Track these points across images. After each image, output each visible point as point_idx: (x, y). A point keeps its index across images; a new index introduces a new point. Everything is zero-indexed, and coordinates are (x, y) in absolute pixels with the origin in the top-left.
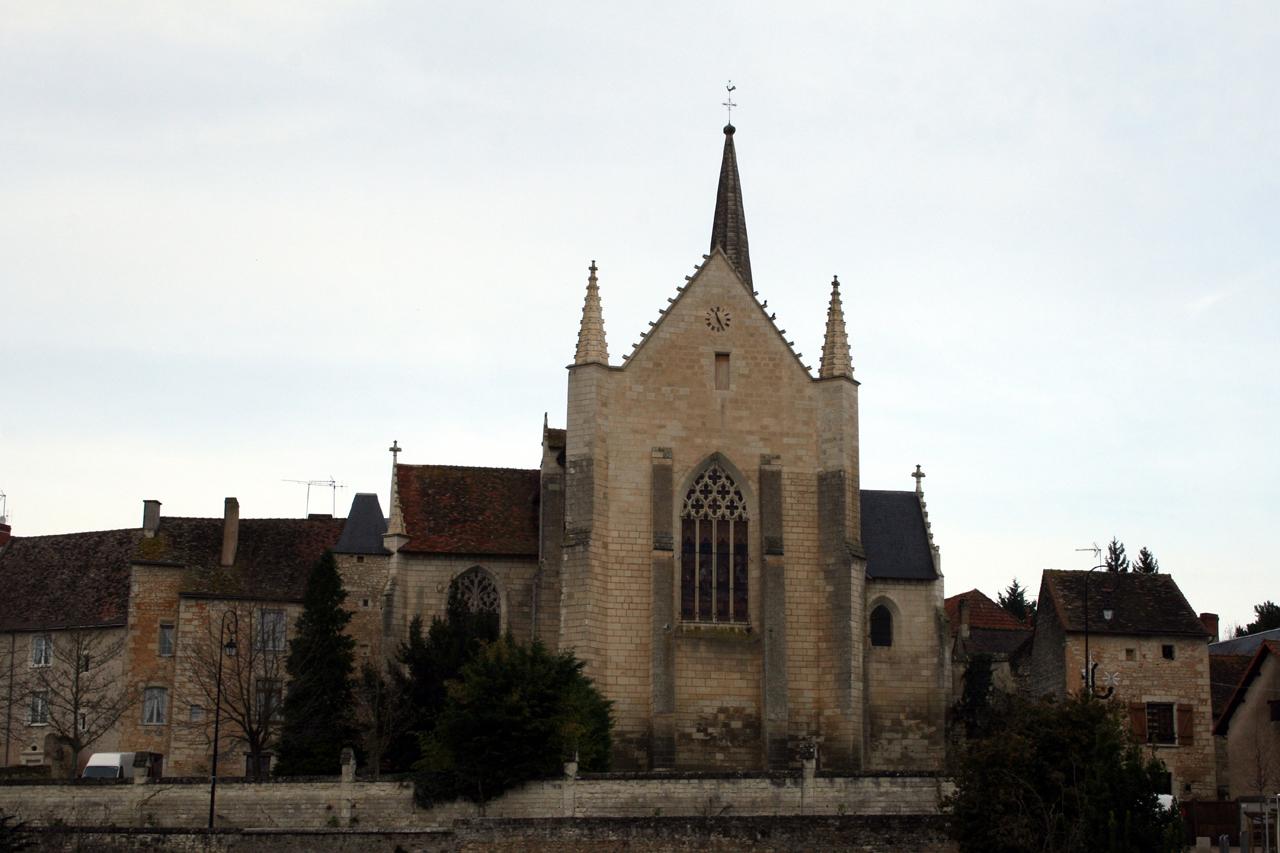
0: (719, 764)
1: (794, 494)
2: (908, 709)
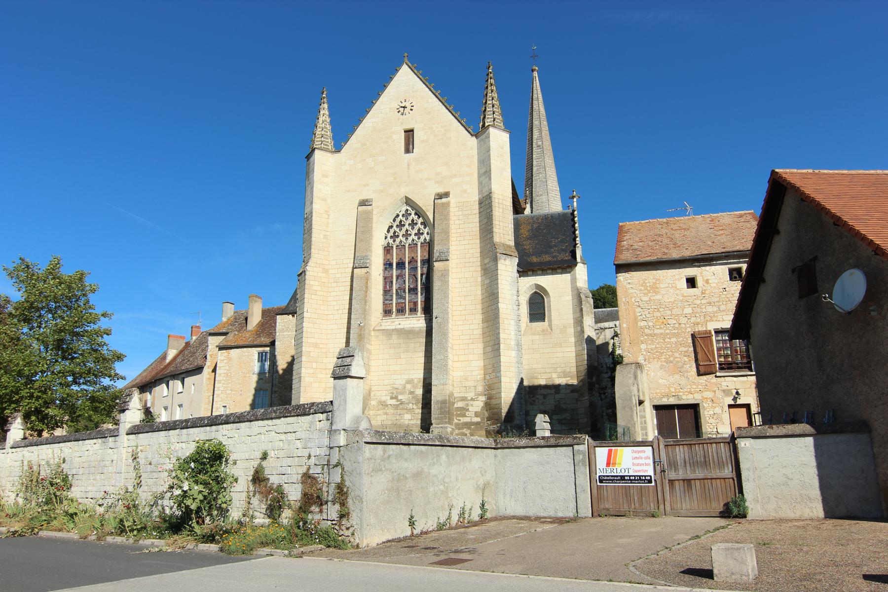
0: (407, 422)
1: (461, 217)
2: (559, 370)
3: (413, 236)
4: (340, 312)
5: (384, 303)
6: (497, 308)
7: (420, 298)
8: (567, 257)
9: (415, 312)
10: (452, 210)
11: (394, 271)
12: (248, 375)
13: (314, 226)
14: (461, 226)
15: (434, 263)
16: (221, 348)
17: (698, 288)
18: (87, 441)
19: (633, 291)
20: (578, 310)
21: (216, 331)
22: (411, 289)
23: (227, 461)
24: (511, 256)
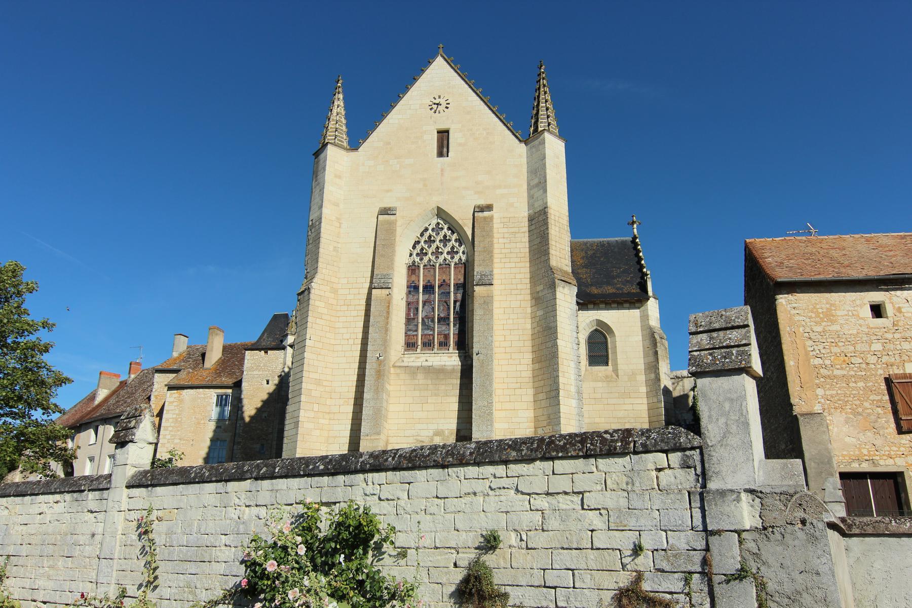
3: (445, 254)
4: (351, 342)
5: (406, 333)
6: (555, 346)
7: (453, 331)
8: (635, 289)
9: (445, 347)
10: (495, 226)
11: (421, 295)
12: (202, 422)
13: (322, 235)
14: (507, 246)
15: (475, 287)
16: (171, 388)
17: (887, 317)
18: (40, 496)
19: (801, 318)
21: (165, 367)
22: (442, 318)
23: (378, 547)
24: (570, 283)
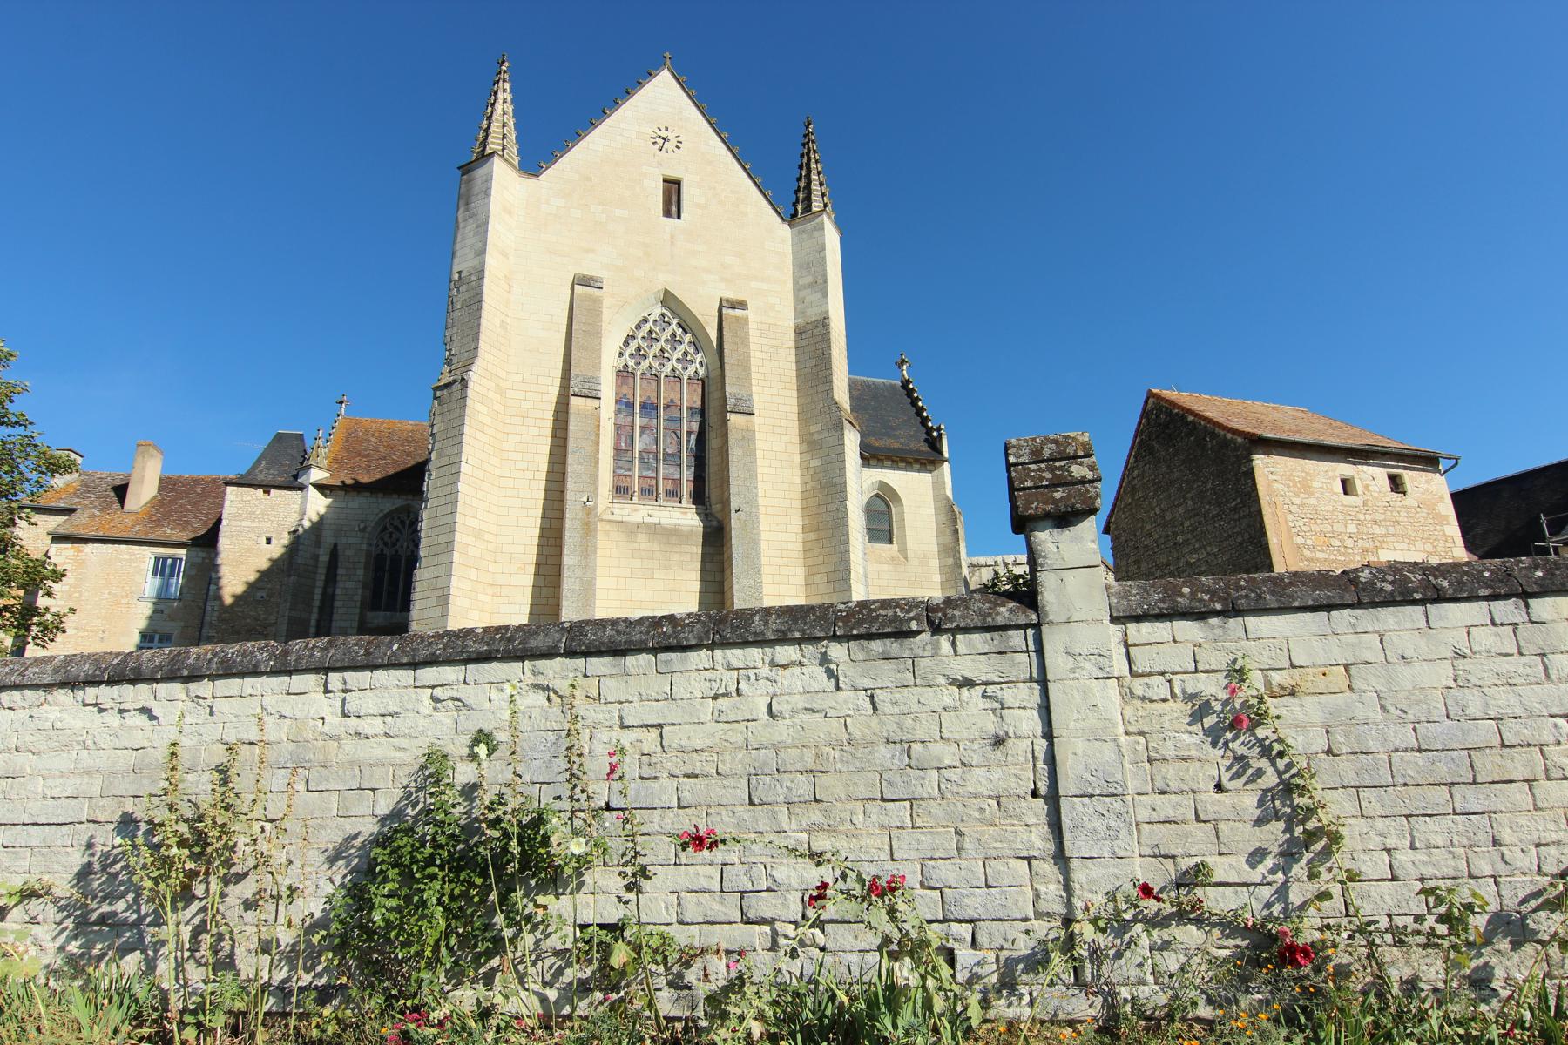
7: (687, 474)
12: (125, 601)
13: (486, 297)
17: (1357, 495)
19: (1280, 486)
20: (948, 531)
